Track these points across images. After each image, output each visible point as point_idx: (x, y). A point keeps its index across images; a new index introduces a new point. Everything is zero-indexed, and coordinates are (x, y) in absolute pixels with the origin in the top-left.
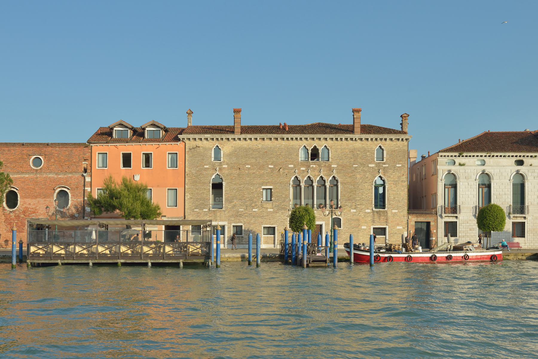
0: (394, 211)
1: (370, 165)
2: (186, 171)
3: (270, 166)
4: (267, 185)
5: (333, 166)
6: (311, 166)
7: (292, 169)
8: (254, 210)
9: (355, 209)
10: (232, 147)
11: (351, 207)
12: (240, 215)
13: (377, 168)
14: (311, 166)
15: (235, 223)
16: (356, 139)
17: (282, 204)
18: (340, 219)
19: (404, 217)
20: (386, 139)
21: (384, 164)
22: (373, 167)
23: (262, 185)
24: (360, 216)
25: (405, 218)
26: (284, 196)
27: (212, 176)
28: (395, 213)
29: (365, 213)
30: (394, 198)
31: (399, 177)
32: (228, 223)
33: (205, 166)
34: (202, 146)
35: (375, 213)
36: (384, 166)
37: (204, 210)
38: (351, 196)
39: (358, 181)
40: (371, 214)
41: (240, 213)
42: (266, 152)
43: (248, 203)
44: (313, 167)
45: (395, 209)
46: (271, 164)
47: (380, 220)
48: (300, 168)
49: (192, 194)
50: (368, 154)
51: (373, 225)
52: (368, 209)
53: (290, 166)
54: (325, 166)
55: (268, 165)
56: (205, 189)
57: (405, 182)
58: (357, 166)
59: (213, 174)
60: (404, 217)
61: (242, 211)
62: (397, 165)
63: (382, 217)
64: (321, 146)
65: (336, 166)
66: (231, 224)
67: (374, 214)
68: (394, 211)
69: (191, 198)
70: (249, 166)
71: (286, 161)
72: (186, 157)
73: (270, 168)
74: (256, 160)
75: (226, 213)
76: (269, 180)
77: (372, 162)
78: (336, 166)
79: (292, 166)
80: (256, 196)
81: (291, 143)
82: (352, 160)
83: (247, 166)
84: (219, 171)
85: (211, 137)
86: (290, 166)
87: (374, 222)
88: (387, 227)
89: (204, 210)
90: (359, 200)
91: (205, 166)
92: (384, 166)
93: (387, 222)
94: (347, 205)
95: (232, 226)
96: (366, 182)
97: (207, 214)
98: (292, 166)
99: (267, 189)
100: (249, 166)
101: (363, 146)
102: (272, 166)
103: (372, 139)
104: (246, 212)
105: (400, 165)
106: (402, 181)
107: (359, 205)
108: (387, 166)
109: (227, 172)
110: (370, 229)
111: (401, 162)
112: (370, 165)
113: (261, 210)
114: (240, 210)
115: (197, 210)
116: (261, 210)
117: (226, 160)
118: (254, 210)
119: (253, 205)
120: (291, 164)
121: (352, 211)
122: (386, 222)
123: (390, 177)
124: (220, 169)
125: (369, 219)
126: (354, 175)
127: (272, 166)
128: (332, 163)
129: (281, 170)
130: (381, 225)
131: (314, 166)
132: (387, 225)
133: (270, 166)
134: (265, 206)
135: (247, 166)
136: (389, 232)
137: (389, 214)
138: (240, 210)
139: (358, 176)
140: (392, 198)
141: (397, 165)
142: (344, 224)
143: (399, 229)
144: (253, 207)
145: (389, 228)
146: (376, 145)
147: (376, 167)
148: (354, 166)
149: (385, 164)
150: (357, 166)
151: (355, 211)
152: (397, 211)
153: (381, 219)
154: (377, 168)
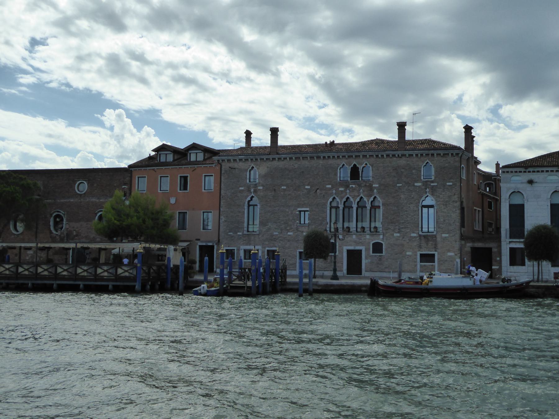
0: (444, 235)
1: (416, 184)
2: (222, 193)
3: (307, 187)
4: (303, 207)
5: (374, 185)
6: (351, 186)
7: (330, 189)
8: (289, 233)
9: (399, 232)
10: (268, 167)
11: (394, 230)
12: (275, 238)
13: (423, 187)
14: (351, 186)
15: (269, 247)
16: (398, 155)
17: (319, 227)
18: (382, 244)
19: (456, 241)
20: (433, 155)
21: (432, 182)
22: (419, 186)
23: (299, 207)
24: (404, 240)
25: (458, 243)
26: (320, 219)
27: (246, 198)
28: (446, 237)
29: (411, 237)
30: (444, 221)
31: (450, 197)
32: (262, 248)
33: (241, 188)
34: (238, 167)
35: (422, 238)
36: (432, 184)
37: (238, 233)
38: (394, 218)
39: (402, 202)
40: (418, 238)
41: (274, 237)
42: (303, 172)
43: (283, 226)
44: (352, 187)
45: (445, 233)
46: (308, 185)
47: (427, 245)
48: (339, 188)
49: (227, 216)
50: (414, 171)
51: (419, 251)
52: (414, 233)
53: (328, 186)
54: (366, 185)
55: (304, 185)
56: (240, 212)
57: (456, 202)
58: (401, 185)
59: (248, 196)
60: (456, 241)
61: (277, 235)
62: (448, 184)
63: (431, 242)
64: (362, 164)
65: (377, 185)
66: (265, 248)
67: (420, 239)
68: (444, 235)
69: (225, 221)
70: (285, 187)
71: (324, 181)
72: (222, 179)
73: (307, 189)
74: (292, 181)
75: (260, 236)
76: (306, 202)
77: (418, 180)
78: (377, 185)
79: (330, 186)
80: (291, 219)
81: (331, 162)
82: (396, 179)
83: (282, 187)
84: (254, 193)
85: (246, 158)
86: (328, 186)
87: (421, 248)
88: (436, 253)
89: (238, 233)
90: (403, 223)
91: (241, 188)
92: (432, 184)
93: (436, 249)
94: (389, 229)
95: (266, 251)
96: (412, 203)
97: (241, 238)
98: (330, 186)
99: (305, 211)
100: (285, 187)
101: (408, 162)
102: (309, 187)
103: (417, 155)
104: (281, 235)
105: (451, 184)
106: (454, 201)
107: (403, 228)
108: (436, 184)
109: (262, 194)
110: (416, 255)
111: (452, 180)
112: (416, 184)
113: (296, 234)
114: (275, 233)
115: (231, 233)
116: (296, 234)
117: (261, 182)
118: (289, 233)
119: (288, 228)
120: (329, 184)
121: (395, 235)
122: (435, 248)
123: (439, 197)
124: (255, 191)
125: (415, 244)
126: (398, 195)
127: (309, 187)
128: (373, 182)
129: (318, 191)
130: (428, 251)
131: (354, 186)
132: (436, 251)
133: (307, 187)
134: (300, 230)
135: (282, 187)
136: (438, 259)
137: (439, 239)
138: (275, 233)
139: (402, 196)
140: (442, 220)
141: (448, 184)
142: (386, 249)
143: (450, 256)
144: (288, 231)
145: (438, 254)
146: (423, 162)
147: (423, 185)
148: (398, 185)
149: (433, 183)
150: (401, 185)
151: (398, 235)
152: (447, 235)
153: (430, 244)
154: (423, 187)
